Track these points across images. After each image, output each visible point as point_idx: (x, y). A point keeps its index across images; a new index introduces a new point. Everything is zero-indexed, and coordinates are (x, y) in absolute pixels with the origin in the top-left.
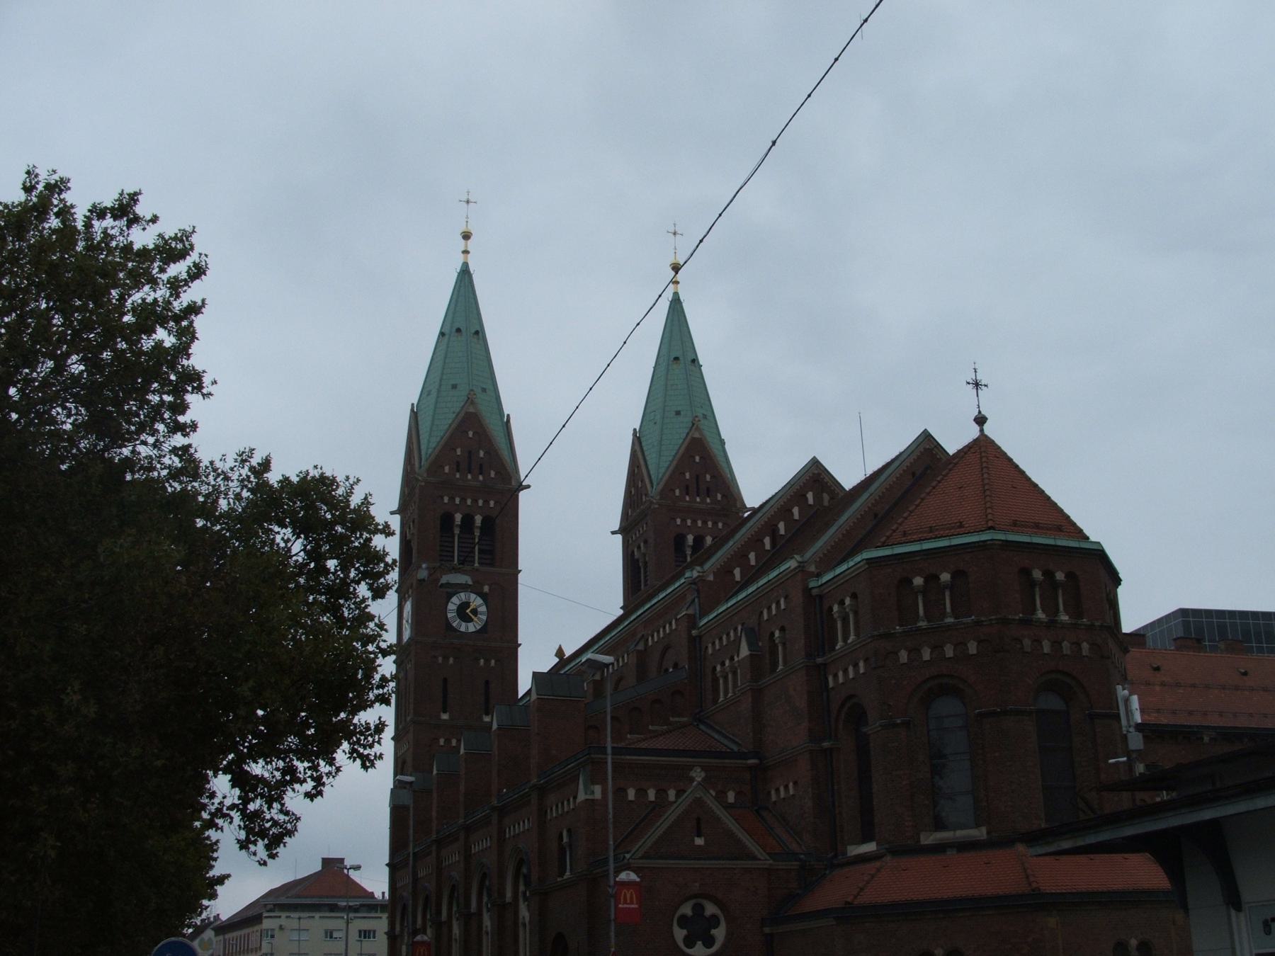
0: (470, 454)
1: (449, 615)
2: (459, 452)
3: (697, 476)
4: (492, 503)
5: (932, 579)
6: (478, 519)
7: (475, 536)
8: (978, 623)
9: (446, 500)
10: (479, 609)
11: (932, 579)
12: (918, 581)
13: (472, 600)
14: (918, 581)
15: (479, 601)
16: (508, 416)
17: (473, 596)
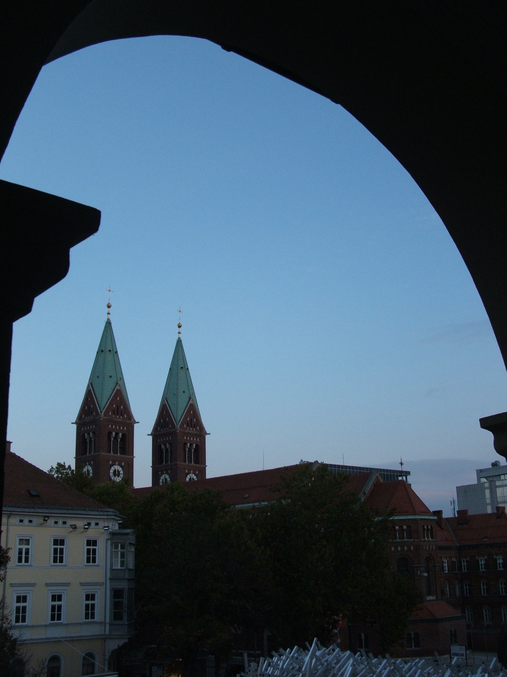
0: (118, 407)
3: (191, 419)
5: (401, 527)
6: (120, 435)
8: (414, 541)
9: (110, 426)
11: (401, 527)
12: (397, 528)
14: (397, 528)
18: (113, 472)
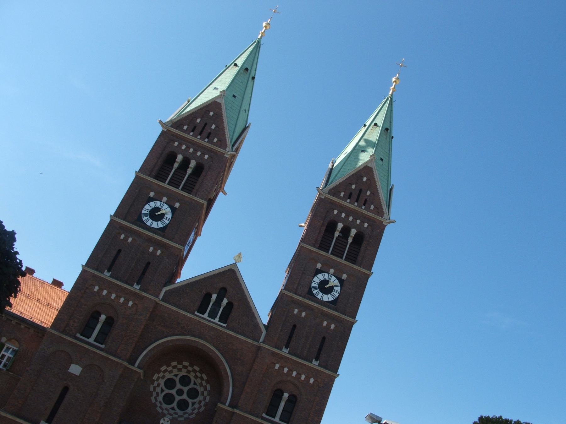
1: (313, 285)
2: (354, 186)
4: (366, 225)
6: (353, 232)
7: (348, 242)
10: (335, 288)
13: (332, 280)
15: (337, 282)
16: (393, 185)
17: (333, 278)
18: (319, 282)
